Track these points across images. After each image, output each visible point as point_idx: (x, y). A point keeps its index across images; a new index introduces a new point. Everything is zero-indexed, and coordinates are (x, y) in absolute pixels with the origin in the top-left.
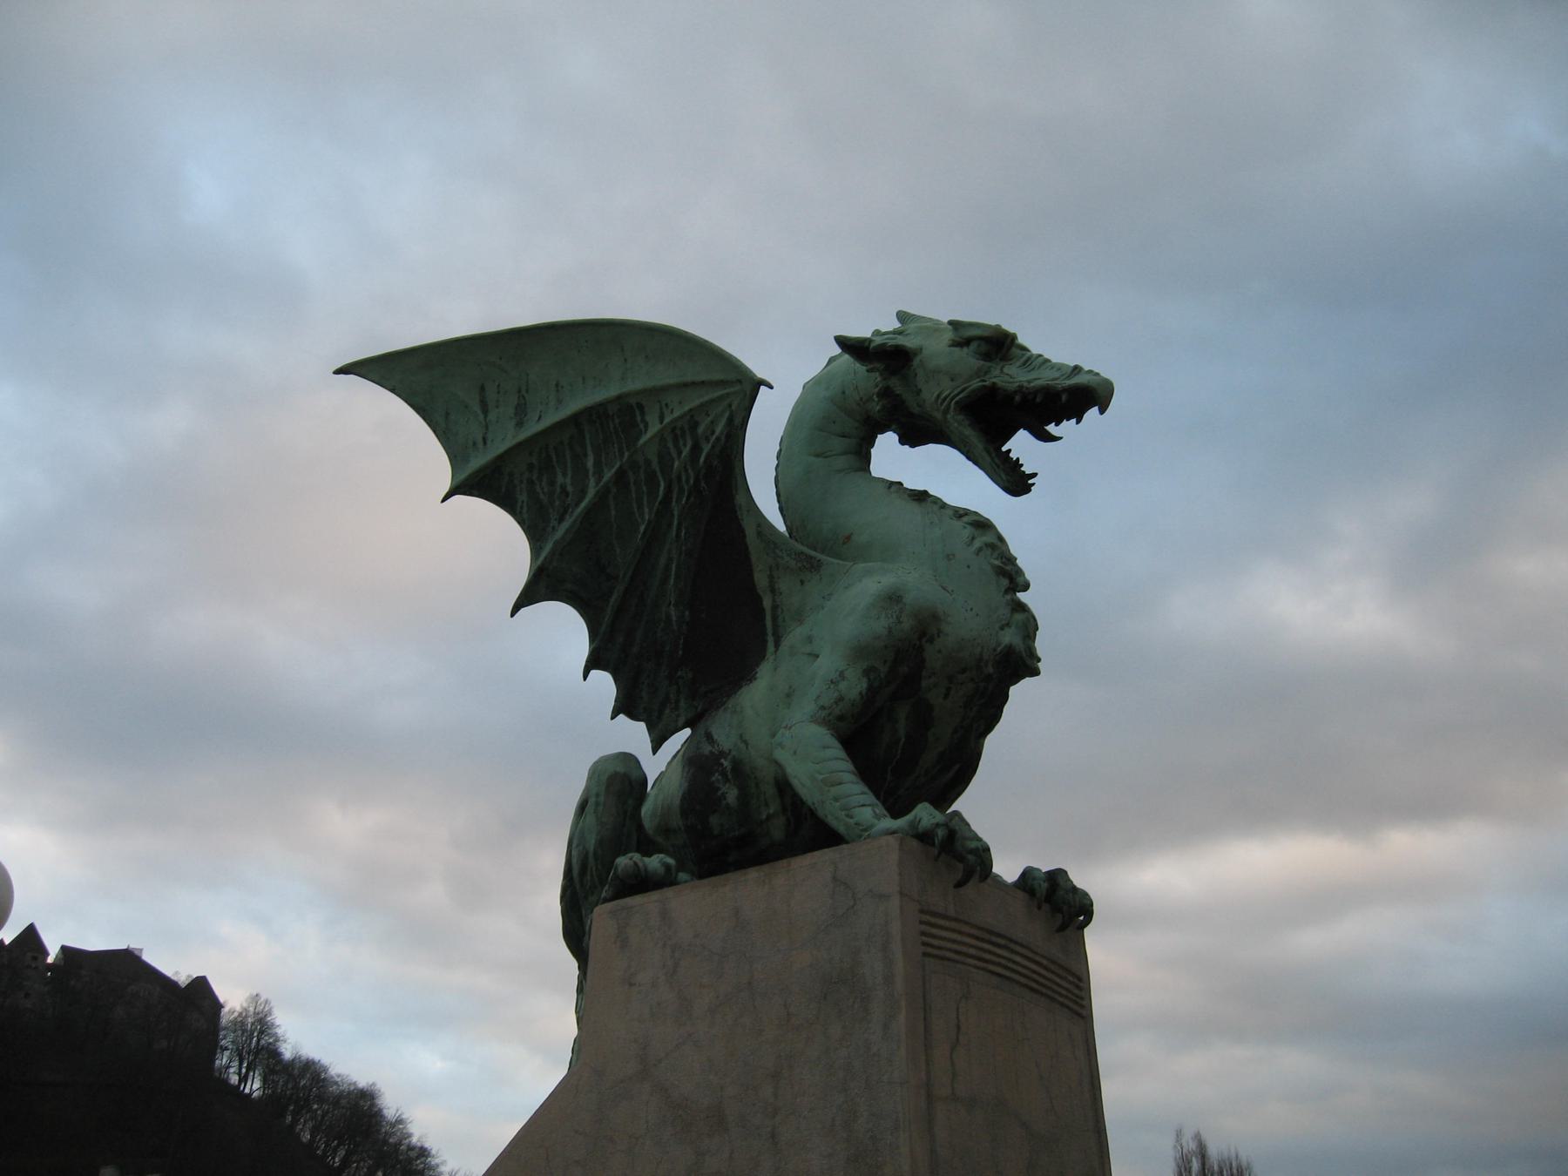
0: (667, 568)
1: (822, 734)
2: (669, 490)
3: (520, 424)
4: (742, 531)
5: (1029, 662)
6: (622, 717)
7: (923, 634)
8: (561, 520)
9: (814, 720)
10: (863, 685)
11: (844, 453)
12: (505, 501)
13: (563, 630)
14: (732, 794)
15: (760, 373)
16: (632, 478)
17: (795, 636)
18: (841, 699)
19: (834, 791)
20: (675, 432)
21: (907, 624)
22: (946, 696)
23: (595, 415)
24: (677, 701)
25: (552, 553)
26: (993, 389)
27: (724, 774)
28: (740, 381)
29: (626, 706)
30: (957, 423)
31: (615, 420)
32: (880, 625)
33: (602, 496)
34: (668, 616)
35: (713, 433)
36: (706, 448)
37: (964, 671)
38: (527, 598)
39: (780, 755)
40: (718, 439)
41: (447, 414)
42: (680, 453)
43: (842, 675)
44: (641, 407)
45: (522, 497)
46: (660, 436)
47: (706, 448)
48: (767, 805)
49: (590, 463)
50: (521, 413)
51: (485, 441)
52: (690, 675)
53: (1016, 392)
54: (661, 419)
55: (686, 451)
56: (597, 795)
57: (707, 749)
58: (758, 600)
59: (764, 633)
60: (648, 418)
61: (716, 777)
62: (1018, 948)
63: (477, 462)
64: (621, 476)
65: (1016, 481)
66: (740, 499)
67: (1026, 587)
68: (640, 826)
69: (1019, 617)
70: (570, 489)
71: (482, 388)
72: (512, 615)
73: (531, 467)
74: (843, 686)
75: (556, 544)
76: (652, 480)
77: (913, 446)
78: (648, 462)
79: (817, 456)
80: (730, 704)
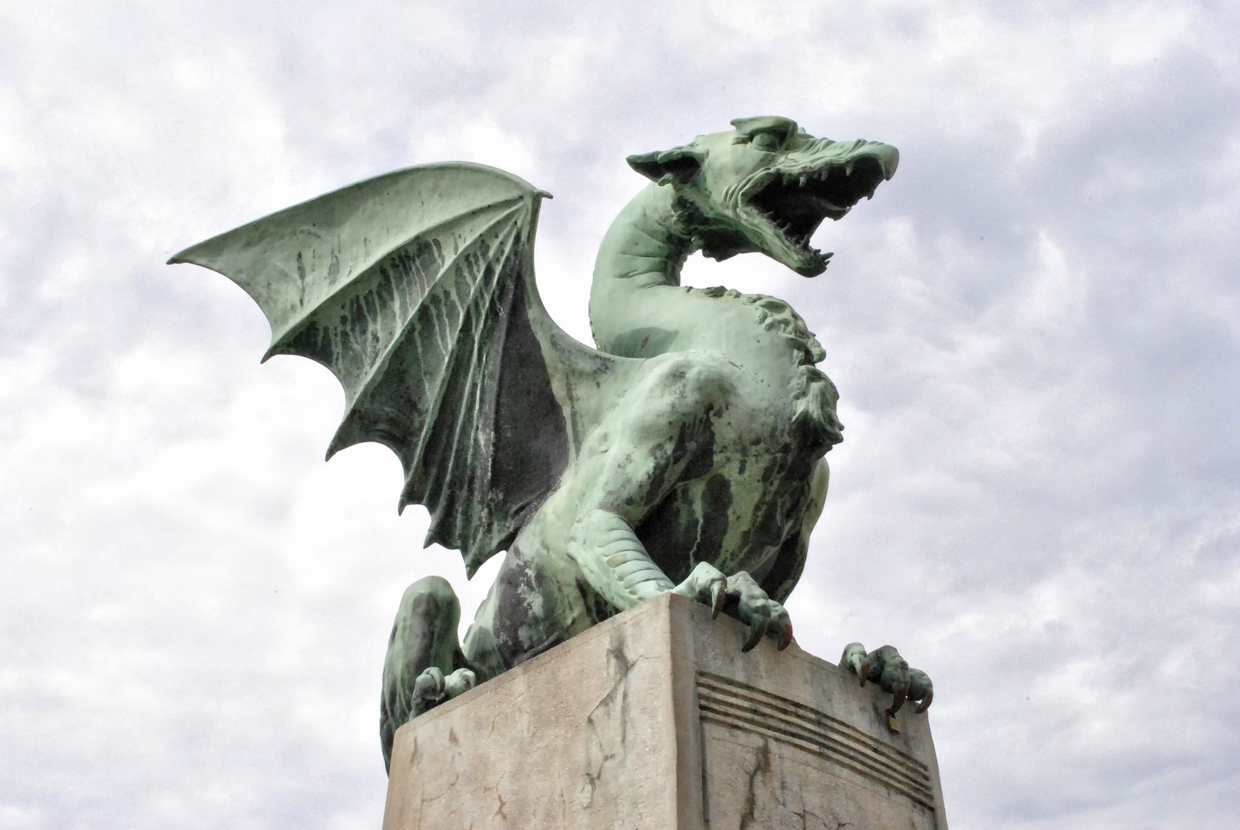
0: (472, 394)
1: (612, 519)
3: (333, 282)
4: (536, 345)
5: (828, 428)
6: (436, 546)
7: (710, 408)
9: (603, 506)
11: (648, 271)
12: (322, 354)
13: (380, 467)
16: (433, 311)
17: (592, 437)
21: (691, 397)
22: (742, 471)
24: (490, 525)
25: (364, 394)
26: (779, 176)
29: (442, 535)
30: (756, 222)
34: (476, 440)
35: (503, 252)
37: (757, 442)
38: (343, 440)
39: (574, 549)
40: (508, 258)
41: (269, 284)
42: (475, 278)
43: (629, 459)
44: (437, 244)
45: (337, 349)
47: (498, 269)
48: (571, 609)
50: (334, 270)
51: (301, 302)
52: (501, 496)
53: (800, 174)
54: (456, 249)
55: (480, 276)
56: (405, 620)
59: (566, 441)
60: (444, 252)
61: (523, 587)
62: (835, 725)
65: (814, 265)
66: (532, 314)
67: (822, 356)
69: (816, 386)
70: (380, 335)
71: (300, 256)
72: (328, 458)
73: (344, 320)
74: (630, 468)
77: (720, 258)
79: (622, 276)
80: (536, 516)
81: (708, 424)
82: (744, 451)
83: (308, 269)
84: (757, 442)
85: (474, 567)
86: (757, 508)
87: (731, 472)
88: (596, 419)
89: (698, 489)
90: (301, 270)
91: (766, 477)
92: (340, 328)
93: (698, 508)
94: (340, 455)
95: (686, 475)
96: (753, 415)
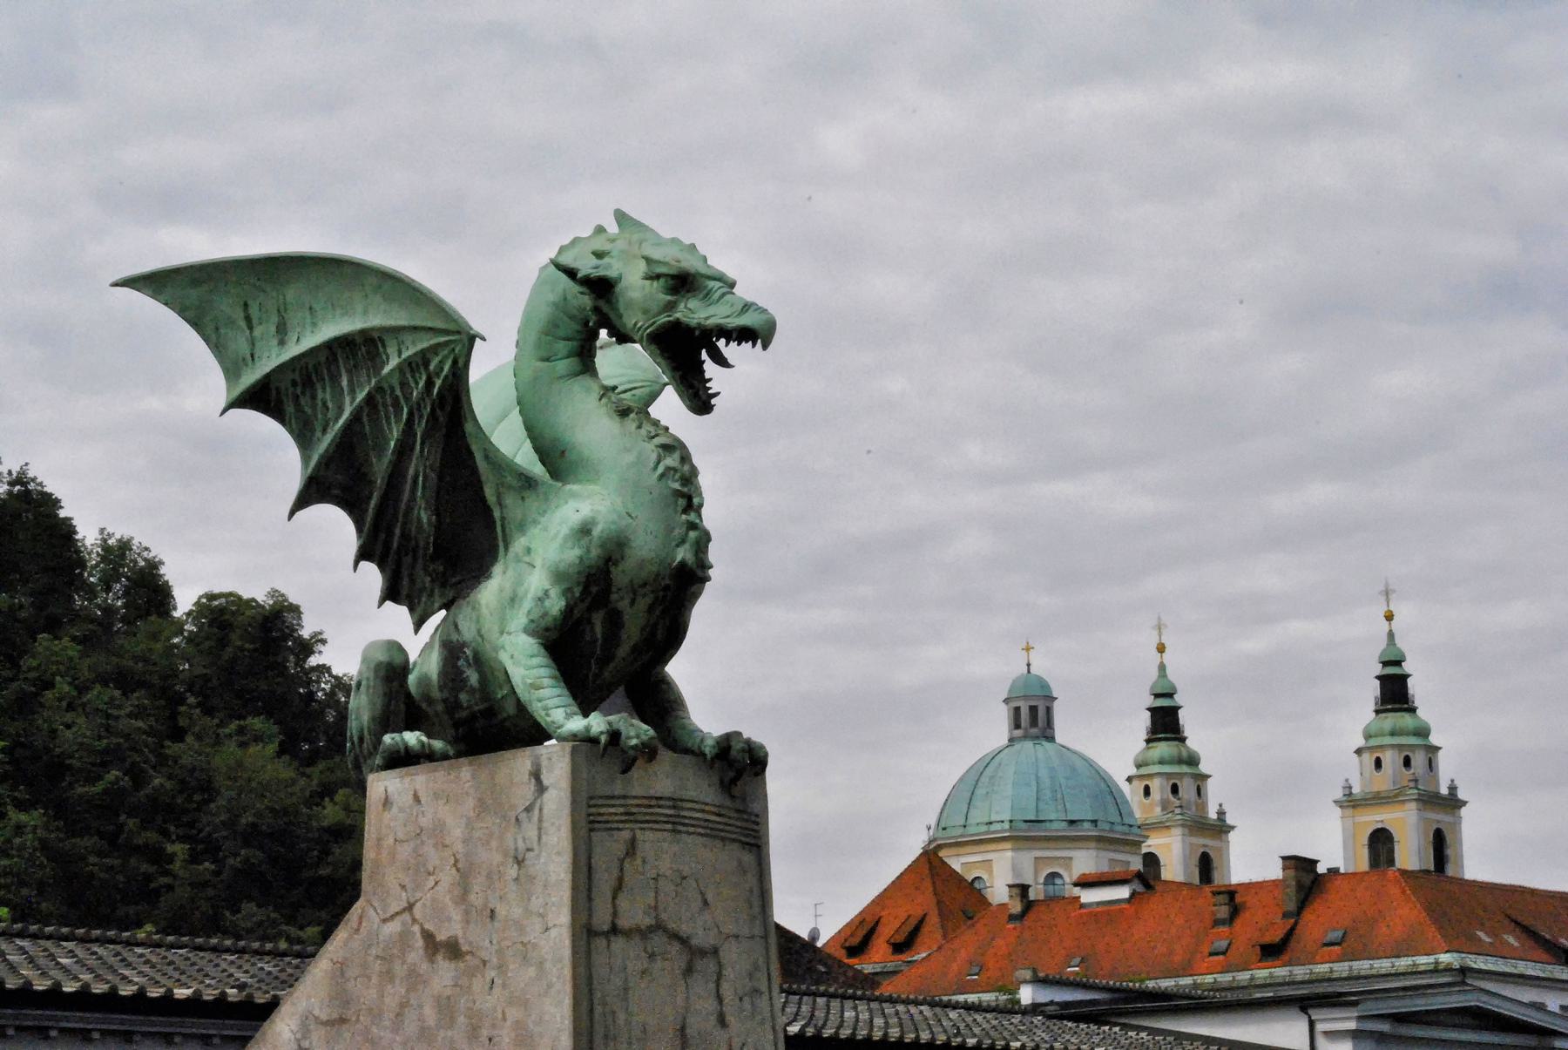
0: (415, 481)
2: (411, 414)
3: (282, 343)
4: (471, 454)
5: (700, 573)
6: (388, 603)
8: (324, 431)
9: (526, 631)
12: (276, 413)
14: (473, 677)
15: (477, 325)
17: (519, 544)
18: (545, 614)
20: (413, 366)
21: (595, 552)
22: (633, 602)
24: (432, 591)
27: (467, 660)
28: (458, 332)
29: (392, 593)
32: (573, 554)
34: (419, 519)
36: (438, 383)
38: (302, 502)
42: (417, 383)
43: (546, 593)
45: (290, 409)
46: (400, 368)
47: (438, 383)
49: (345, 383)
50: (282, 331)
55: (422, 384)
57: (455, 637)
58: (488, 511)
59: (496, 538)
60: (389, 350)
61: (461, 662)
63: (250, 378)
64: (370, 399)
68: (408, 695)
69: (693, 534)
71: (246, 305)
73: (294, 384)
74: (547, 603)
75: (322, 456)
76: (396, 404)
78: (392, 389)
81: (608, 572)
83: (255, 321)
84: (645, 584)
85: (418, 625)
86: (643, 629)
87: (623, 605)
88: (522, 528)
89: (598, 619)
90: (248, 319)
91: (651, 609)
92: (291, 390)
93: (598, 629)
94: (300, 514)
95: (591, 609)
96: (642, 564)
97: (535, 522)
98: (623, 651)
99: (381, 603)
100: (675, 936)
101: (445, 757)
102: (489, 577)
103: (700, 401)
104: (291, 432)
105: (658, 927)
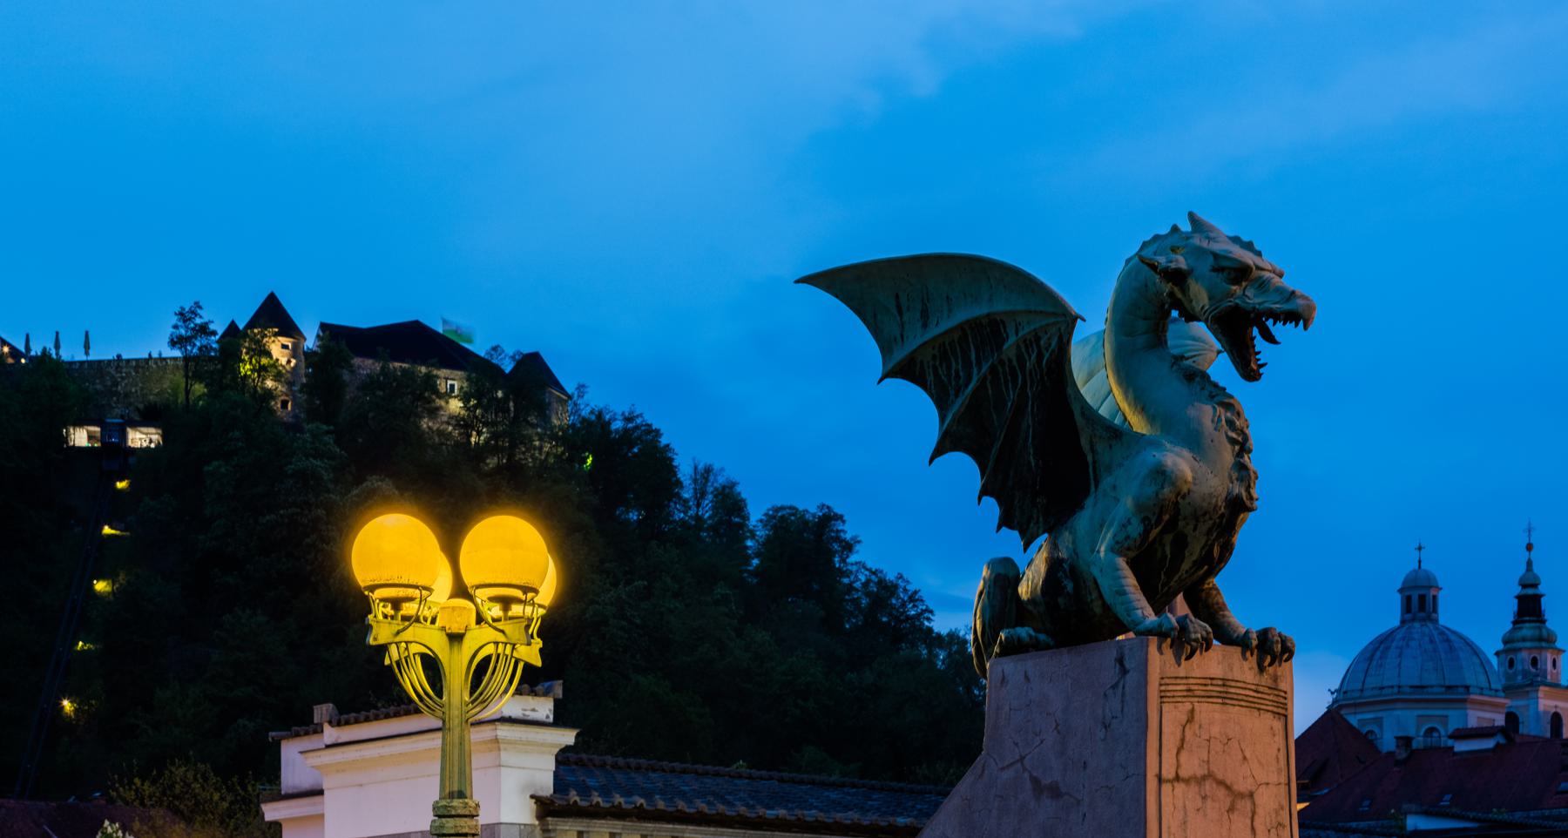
2: (1024, 381)
3: (925, 326)
5: (1248, 503)
8: (957, 396)
10: (1141, 528)
13: (963, 468)
14: (1070, 586)
17: (1106, 482)
18: (1128, 537)
19: (1121, 599)
23: (974, 325)
25: (953, 420)
29: (1006, 521)
31: (988, 332)
33: (983, 382)
36: (1047, 355)
38: (939, 451)
43: (1129, 522)
45: (930, 378)
47: (1047, 355)
50: (925, 316)
55: (1034, 356)
63: (900, 354)
64: (993, 369)
66: (1070, 391)
71: (897, 296)
73: (934, 357)
74: (1129, 528)
78: (1010, 360)
82: (1197, 520)
87: (1189, 530)
88: (1109, 469)
89: (1168, 538)
91: (1209, 532)
97: (1120, 465)
98: (1186, 566)
99: (999, 528)
100: (1221, 783)
101: (1048, 647)
102: (1082, 508)
103: (1250, 372)
104: (931, 396)
105: (1209, 776)
